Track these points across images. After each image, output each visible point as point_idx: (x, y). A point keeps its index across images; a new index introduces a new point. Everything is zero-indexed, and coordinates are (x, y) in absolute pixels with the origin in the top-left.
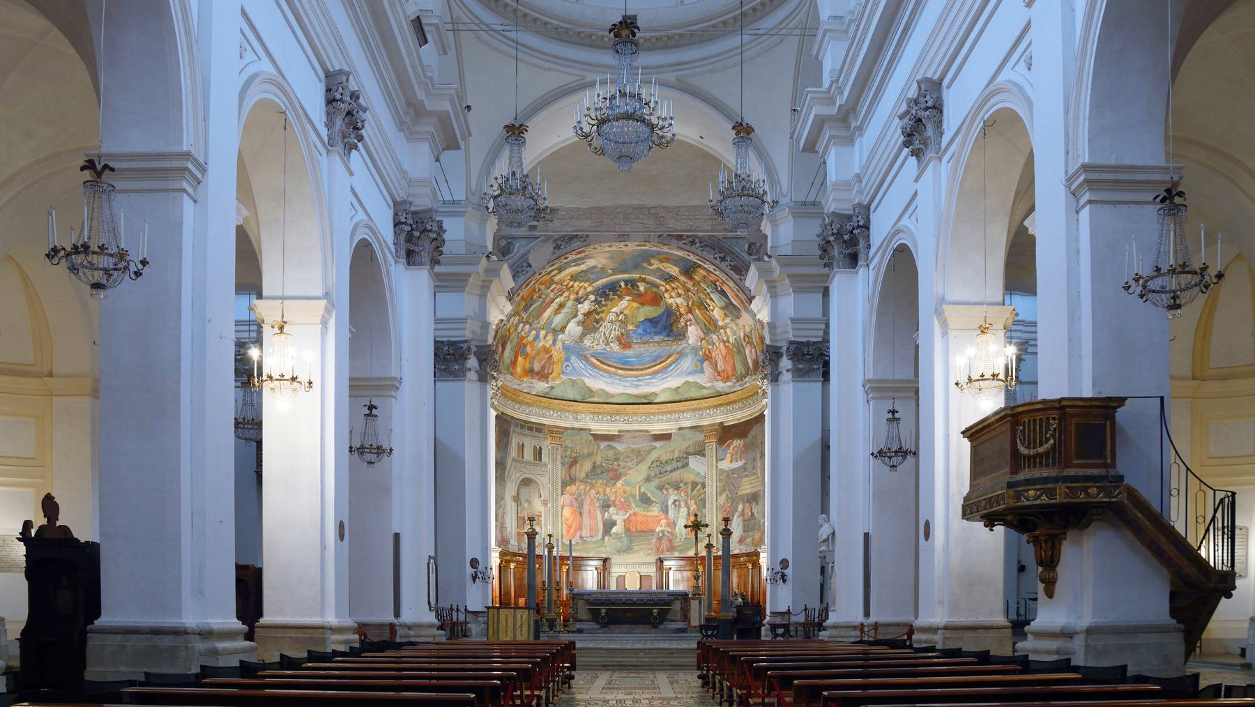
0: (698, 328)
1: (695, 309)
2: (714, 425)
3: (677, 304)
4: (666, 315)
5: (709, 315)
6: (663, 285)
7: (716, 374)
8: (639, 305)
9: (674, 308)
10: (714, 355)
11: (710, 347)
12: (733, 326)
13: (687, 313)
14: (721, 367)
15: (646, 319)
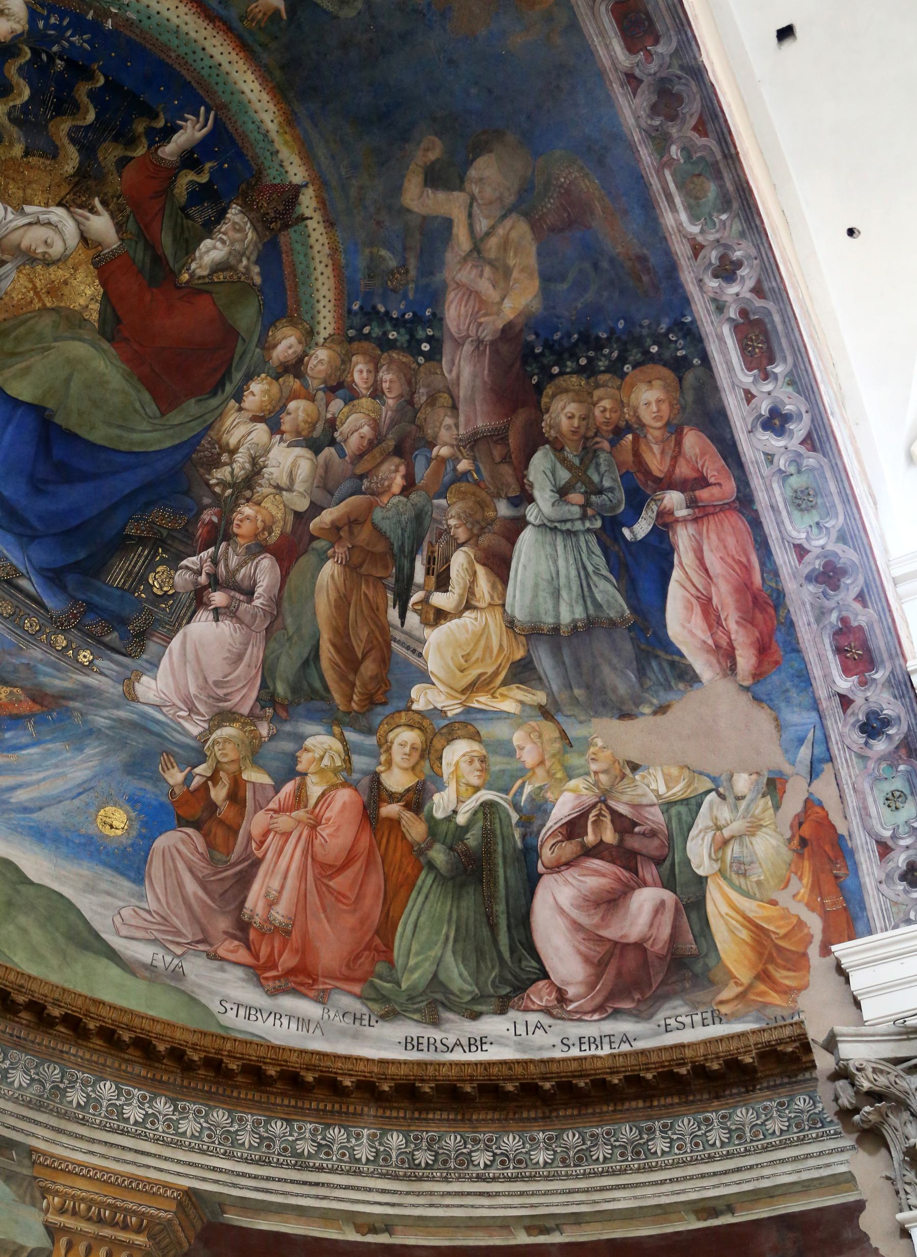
0: (255, 653)
1: (323, 559)
2: (134, 1185)
3: (256, 469)
4: (141, 475)
5: (383, 628)
6: (310, 333)
7: (223, 924)
8: (93, 314)
9: (223, 473)
10: (256, 823)
11: (254, 776)
12: (518, 738)
13: (258, 548)
14: (271, 904)
15: (45, 409)
